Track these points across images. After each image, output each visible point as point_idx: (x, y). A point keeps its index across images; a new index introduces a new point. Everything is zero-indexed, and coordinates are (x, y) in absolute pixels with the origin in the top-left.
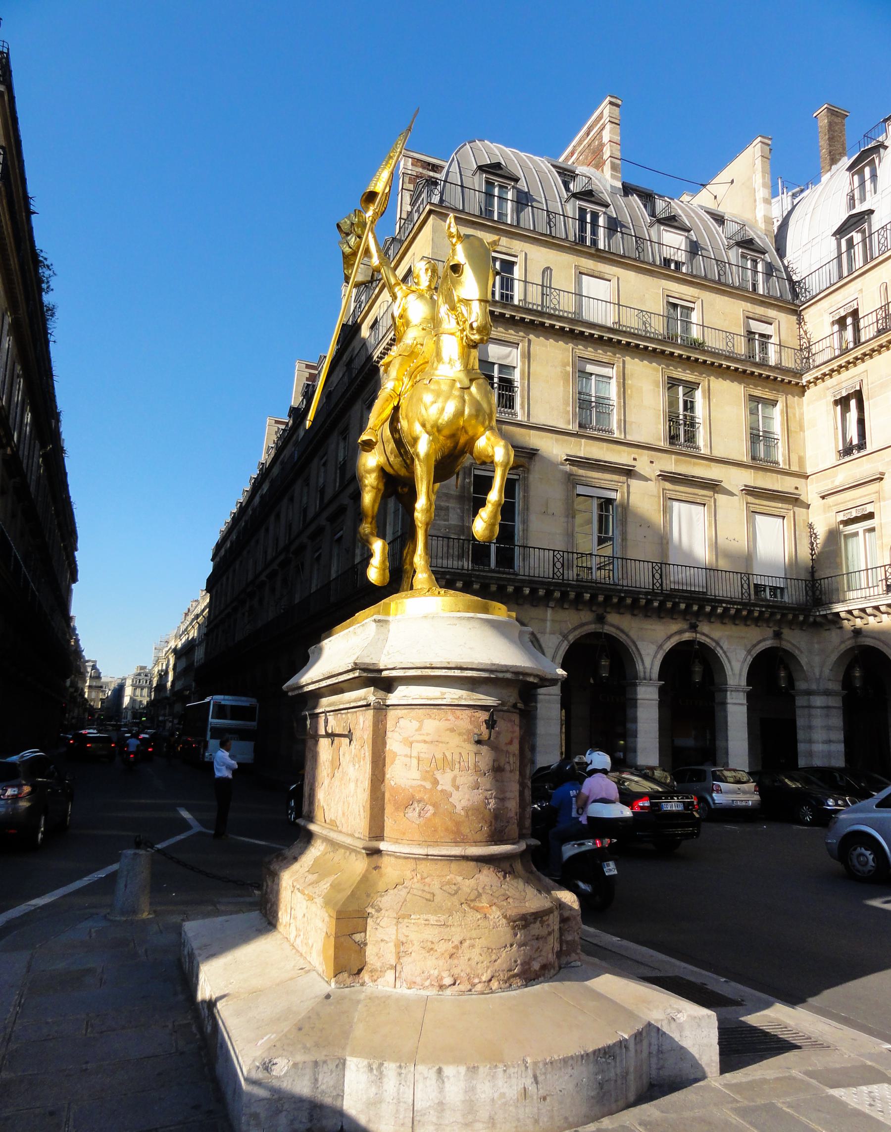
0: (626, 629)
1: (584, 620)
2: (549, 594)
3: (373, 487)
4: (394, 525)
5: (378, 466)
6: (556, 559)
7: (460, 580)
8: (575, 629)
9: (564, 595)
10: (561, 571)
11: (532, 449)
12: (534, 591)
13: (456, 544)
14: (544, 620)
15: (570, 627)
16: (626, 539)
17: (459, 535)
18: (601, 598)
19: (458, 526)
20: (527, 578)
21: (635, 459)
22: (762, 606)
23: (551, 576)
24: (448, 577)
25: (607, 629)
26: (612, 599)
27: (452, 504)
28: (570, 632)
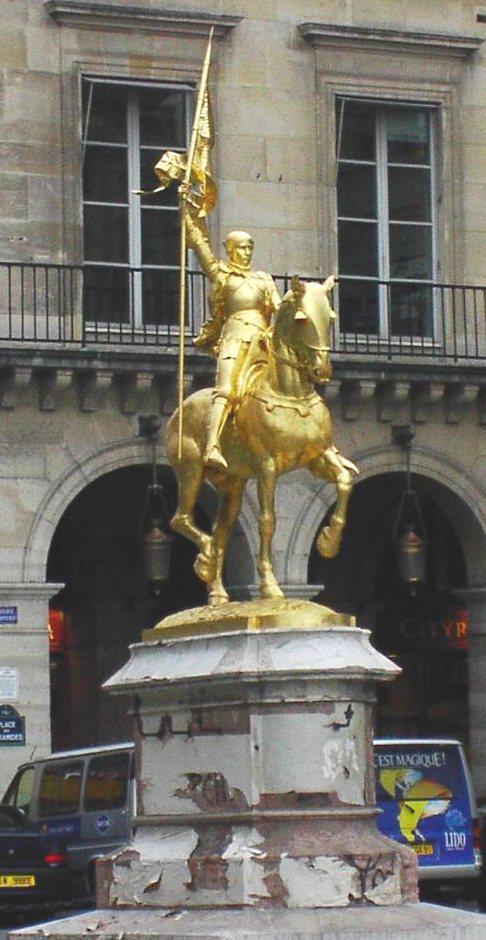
11: (224, 17)
16: (462, 231)
18: (402, 390)
24: (37, 362)
25: (419, 464)
26: (428, 392)
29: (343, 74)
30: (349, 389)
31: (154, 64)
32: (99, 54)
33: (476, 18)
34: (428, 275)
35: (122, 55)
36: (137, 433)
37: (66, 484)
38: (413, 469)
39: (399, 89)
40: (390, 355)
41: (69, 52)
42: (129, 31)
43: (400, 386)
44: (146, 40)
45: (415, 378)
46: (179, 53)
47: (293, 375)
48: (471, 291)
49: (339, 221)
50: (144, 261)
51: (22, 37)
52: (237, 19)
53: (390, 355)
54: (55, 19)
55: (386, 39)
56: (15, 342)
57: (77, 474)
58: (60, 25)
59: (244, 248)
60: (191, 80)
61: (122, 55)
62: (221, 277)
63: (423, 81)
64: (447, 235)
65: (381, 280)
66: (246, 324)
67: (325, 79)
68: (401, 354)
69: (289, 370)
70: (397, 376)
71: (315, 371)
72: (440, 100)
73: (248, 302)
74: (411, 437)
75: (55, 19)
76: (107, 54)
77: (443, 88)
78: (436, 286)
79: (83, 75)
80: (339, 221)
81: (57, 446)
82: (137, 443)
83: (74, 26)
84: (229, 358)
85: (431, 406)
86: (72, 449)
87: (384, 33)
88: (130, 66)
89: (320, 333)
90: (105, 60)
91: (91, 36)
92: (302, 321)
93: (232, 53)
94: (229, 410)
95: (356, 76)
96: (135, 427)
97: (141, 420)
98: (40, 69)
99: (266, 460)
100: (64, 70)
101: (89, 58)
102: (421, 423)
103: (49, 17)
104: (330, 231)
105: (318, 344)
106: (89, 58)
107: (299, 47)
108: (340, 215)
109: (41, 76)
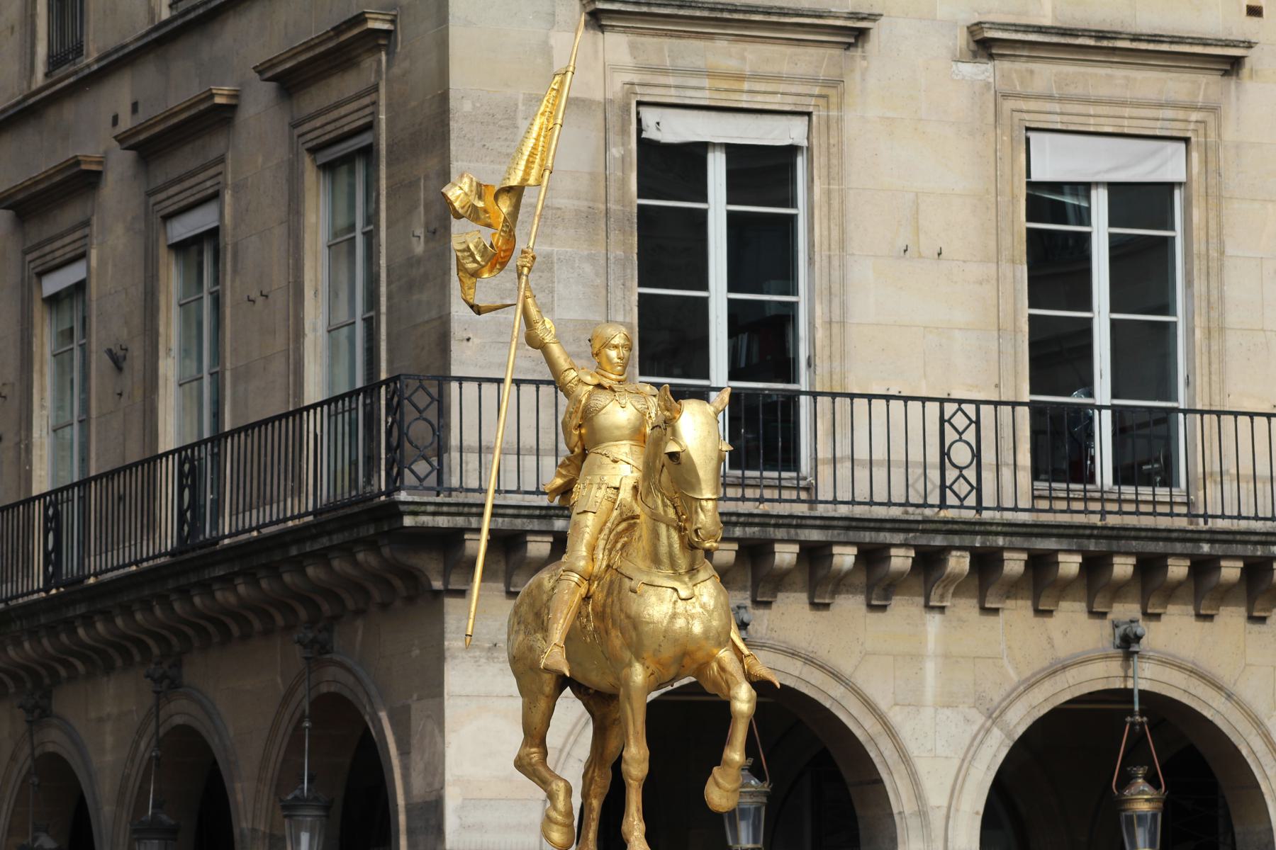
0: (1225, 674)
1: (1064, 649)
2: (929, 561)
4: (333, 293)
6: (950, 435)
8: (1030, 684)
9: (986, 563)
10: (971, 474)
11: (855, 16)
12: (872, 556)
14: (916, 657)
15: (1014, 677)
16: (1222, 329)
18: (1123, 567)
20: (843, 510)
21: (1254, 11)
23: (934, 499)
28: (1013, 697)
29: (1038, 97)
30: (754, 555)
31: (746, 86)
32: (664, 71)
33: (1245, 10)
34: (1170, 394)
35: (696, 73)
38: (1144, 685)
39: (1124, 118)
40: (1103, 513)
41: (616, 69)
42: (710, 36)
44: (737, 48)
45: (923, 540)
46: (786, 69)
47: (669, 537)
48: (828, 400)
49: (640, 295)
50: (732, 377)
52: (873, 17)
53: (1103, 513)
54: (596, 20)
55: (1105, 43)
56: (527, 496)
58: (602, 28)
59: (616, 347)
60: (805, 109)
61: (696, 73)
62: (583, 392)
63: (1160, 106)
64: (1198, 334)
65: (714, 385)
66: (615, 461)
67: (1009, 104)
68: (1120, 512)
69: (663, 529)
70: (1115, 545)
71: (696, 531)
72: (1188, 134)
73: (618, 428)
74: (1138, 638)
75: (596, 20)
76: (675, 71)
77: (1194, 116)
78: (806, 393)
79: (639, 103)
80: (640, 295)
83: (626, 30)
84: (585, 512)
85: (1171, 593)
87: (1101, 35)
89: (701, 473)
90: (671, 80)
91: (650, 42)
92: (673, 456)
93: (866, 69)
94: (583, 591)
95: (1061, 99)
99: (630, 665)
100: (609, 96)
101: (648, 78)
102: (1157, 617)
104: (1016, 330)
105: (701, 490)
106: (648, 78)
107: (975, 56)
108: (1031, 306)
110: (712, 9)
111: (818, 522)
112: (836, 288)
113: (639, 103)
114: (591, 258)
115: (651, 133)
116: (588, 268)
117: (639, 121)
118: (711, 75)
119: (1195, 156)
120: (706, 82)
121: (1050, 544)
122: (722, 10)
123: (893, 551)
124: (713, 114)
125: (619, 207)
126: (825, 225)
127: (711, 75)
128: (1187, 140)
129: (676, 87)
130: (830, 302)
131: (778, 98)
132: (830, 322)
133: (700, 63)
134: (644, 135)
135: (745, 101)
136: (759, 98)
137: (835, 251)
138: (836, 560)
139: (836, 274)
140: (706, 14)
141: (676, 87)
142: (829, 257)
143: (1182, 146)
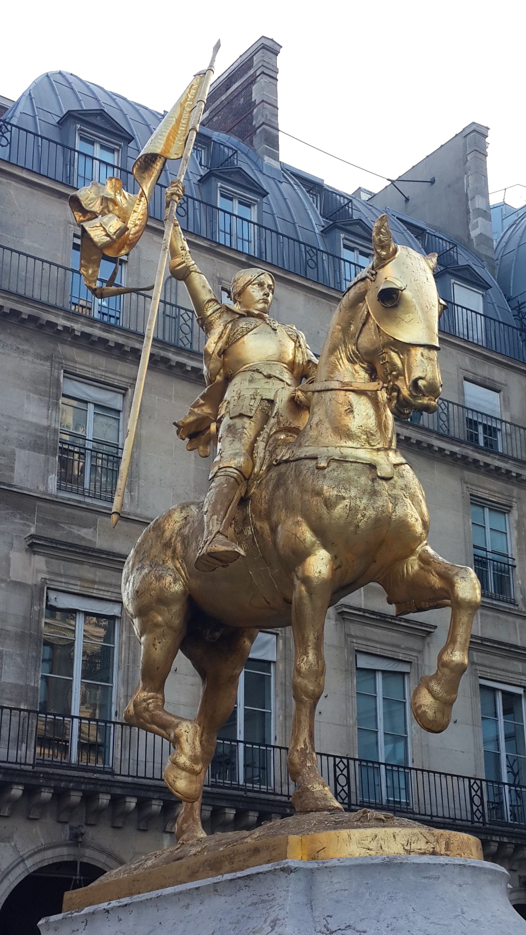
3: (171, 627)
5: (184, 593)
7: (18, 784)
13: (15, 719)
17: (19, 702)
19: (16, 686)
22: (502, 834)
27: (8, 648)
32: (61, 575)
36: (68, 838)
37: (12, 873)
42: (81, 563)
43: (251, 813)
44: (93, 569)
51: (8, 559)
57: (22, 865)
58: (35, 553)
72: (278, 632)
79: (48, 588)
81: (8, 845)
82: (67, 845)
83: (44, 555)
86: (19, 846)
88: (80, 586)
90: (63, 580)
96: (65, 833)
97: (71, 828)
98: (19, 580)
101: (53, 577)
103: (27, 547)
106: (53, 577)
109: (18, 585)
110: (84, 549)
111: (121, 785)
112: (130, 681)
113: (48, 588)
114: (21, 655)
115: (52, 603)
116: (19, 659)
117: (47, 597)
118: (81, 579)
119: (281, 641)
120: (79, 583)
121: (223, 804)
122: (88, 551)
123: (154, 802)
124: (80, 598)
125: (35, 633)
126: (127, 652)
127: (81, 579)
128: (277, 634)
129: (65, 583)
130: (128, 687)
131: (109, 594)
132: (127, 696)
133: (76, 574)
134: (49, 603)
135: (95, 593)
136: (101, 593)
137: (131, 664)
138: (127, 804)
139: (131, 674)
140: (81, 551)
141: (65, 583)
142: (128, 666)
143: (275, 636)
